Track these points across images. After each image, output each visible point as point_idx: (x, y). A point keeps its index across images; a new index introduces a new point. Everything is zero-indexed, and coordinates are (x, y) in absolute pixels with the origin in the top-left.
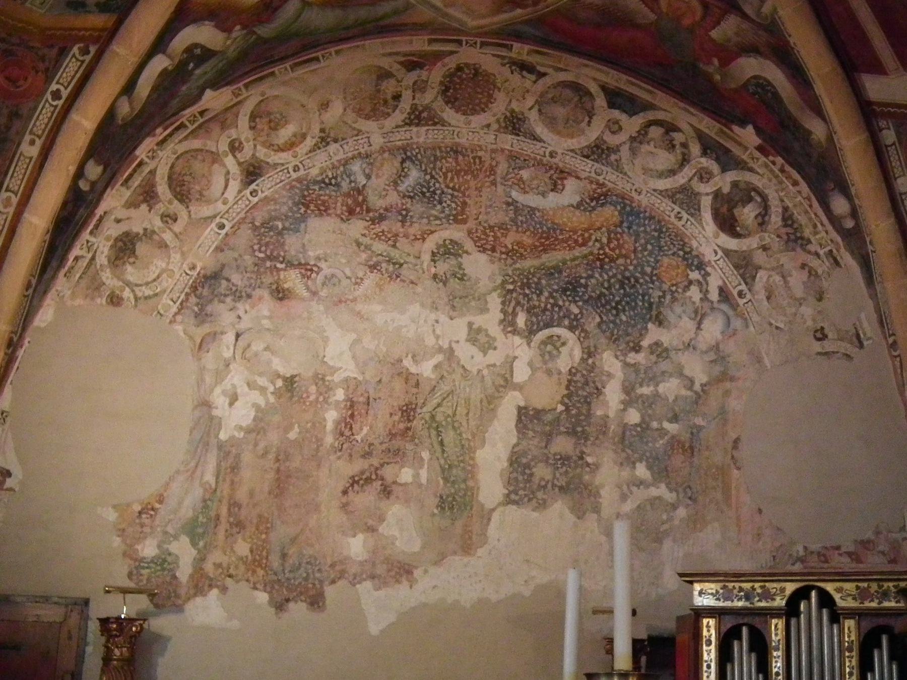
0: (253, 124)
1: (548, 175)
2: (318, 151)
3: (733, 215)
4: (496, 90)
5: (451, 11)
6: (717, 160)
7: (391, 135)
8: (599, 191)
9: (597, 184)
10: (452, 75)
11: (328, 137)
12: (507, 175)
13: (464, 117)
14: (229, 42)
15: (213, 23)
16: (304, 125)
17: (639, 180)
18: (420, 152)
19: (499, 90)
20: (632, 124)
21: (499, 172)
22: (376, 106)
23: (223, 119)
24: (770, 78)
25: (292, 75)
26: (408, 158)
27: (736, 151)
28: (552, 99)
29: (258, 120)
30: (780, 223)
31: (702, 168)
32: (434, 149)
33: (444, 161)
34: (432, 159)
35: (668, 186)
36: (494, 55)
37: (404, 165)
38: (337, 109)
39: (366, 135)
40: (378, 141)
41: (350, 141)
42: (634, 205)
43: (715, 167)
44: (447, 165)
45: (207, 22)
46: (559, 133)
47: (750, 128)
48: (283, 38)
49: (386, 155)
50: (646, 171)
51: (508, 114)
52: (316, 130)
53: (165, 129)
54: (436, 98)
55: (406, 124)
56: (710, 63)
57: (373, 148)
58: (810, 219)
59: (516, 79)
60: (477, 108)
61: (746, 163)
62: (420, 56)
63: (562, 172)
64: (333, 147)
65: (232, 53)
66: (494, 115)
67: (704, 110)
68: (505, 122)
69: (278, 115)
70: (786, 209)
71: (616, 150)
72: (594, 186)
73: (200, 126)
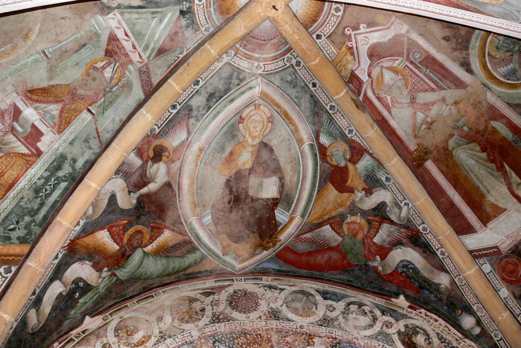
0: (117, 334)
1: (303, 338)
2: (160, 344)
3: (412, 342)
4: (259, 300)
5: (228, 259)
6: (391, 316)
7: (203, 329)
8: (334, 342)
9: (332, 338)
10: (232, 296)
11: (165, 335)
12: (279, 341)
13: (245, 315)
14: (100, 280)
15: (91, 264)
16: (149, 331)
17: (355, 333)
18: (223, 336)
19: (261, 299)
20: (340, 306)
21: (273, 340)
22: (191, 315)
23: (97, 333)
24: (409, 259)
25: (138, 306)
26: (216, 340)
27: (400, 311)
28: (292, 299)
29: (119, 331)
30: (439, 342)
31: (385, 321)
32: (231, 333)
33: (239, 339)
34: (232, 339)
35: (372, 333)
36: (253, 284)
37: (215, 345)
38: (168, 319)
39: (188, 331)
40: (196, 334)
41: (179, 336)
42: (357, 346)
43: (392, 320)
44: (242, 341)
45: (87, 262)
46: (301, 316)
47: (402, 297)
48: (134, 279)
49: (203, 341)
50: (356, 327)
51: (270, 311)
52: (156, 332)
53: (60, 343)
54: (226, 307)
55: (212, 323)
56: (375, 260)
57: (194, 338)
58: (453, 337)
59: (269, 294)
60: (251, 309)
61: (407, 315)
62: (212, 289)
63: (310, 335)
64: (169, 341)
65: (102, 290)
66: (262, 312)
67: (374, 293)
68: (269, 314)
69: (132, 328)
70: (438, 334)
71: (336, 319)
72: (331, 340)
73: (83, 339)
